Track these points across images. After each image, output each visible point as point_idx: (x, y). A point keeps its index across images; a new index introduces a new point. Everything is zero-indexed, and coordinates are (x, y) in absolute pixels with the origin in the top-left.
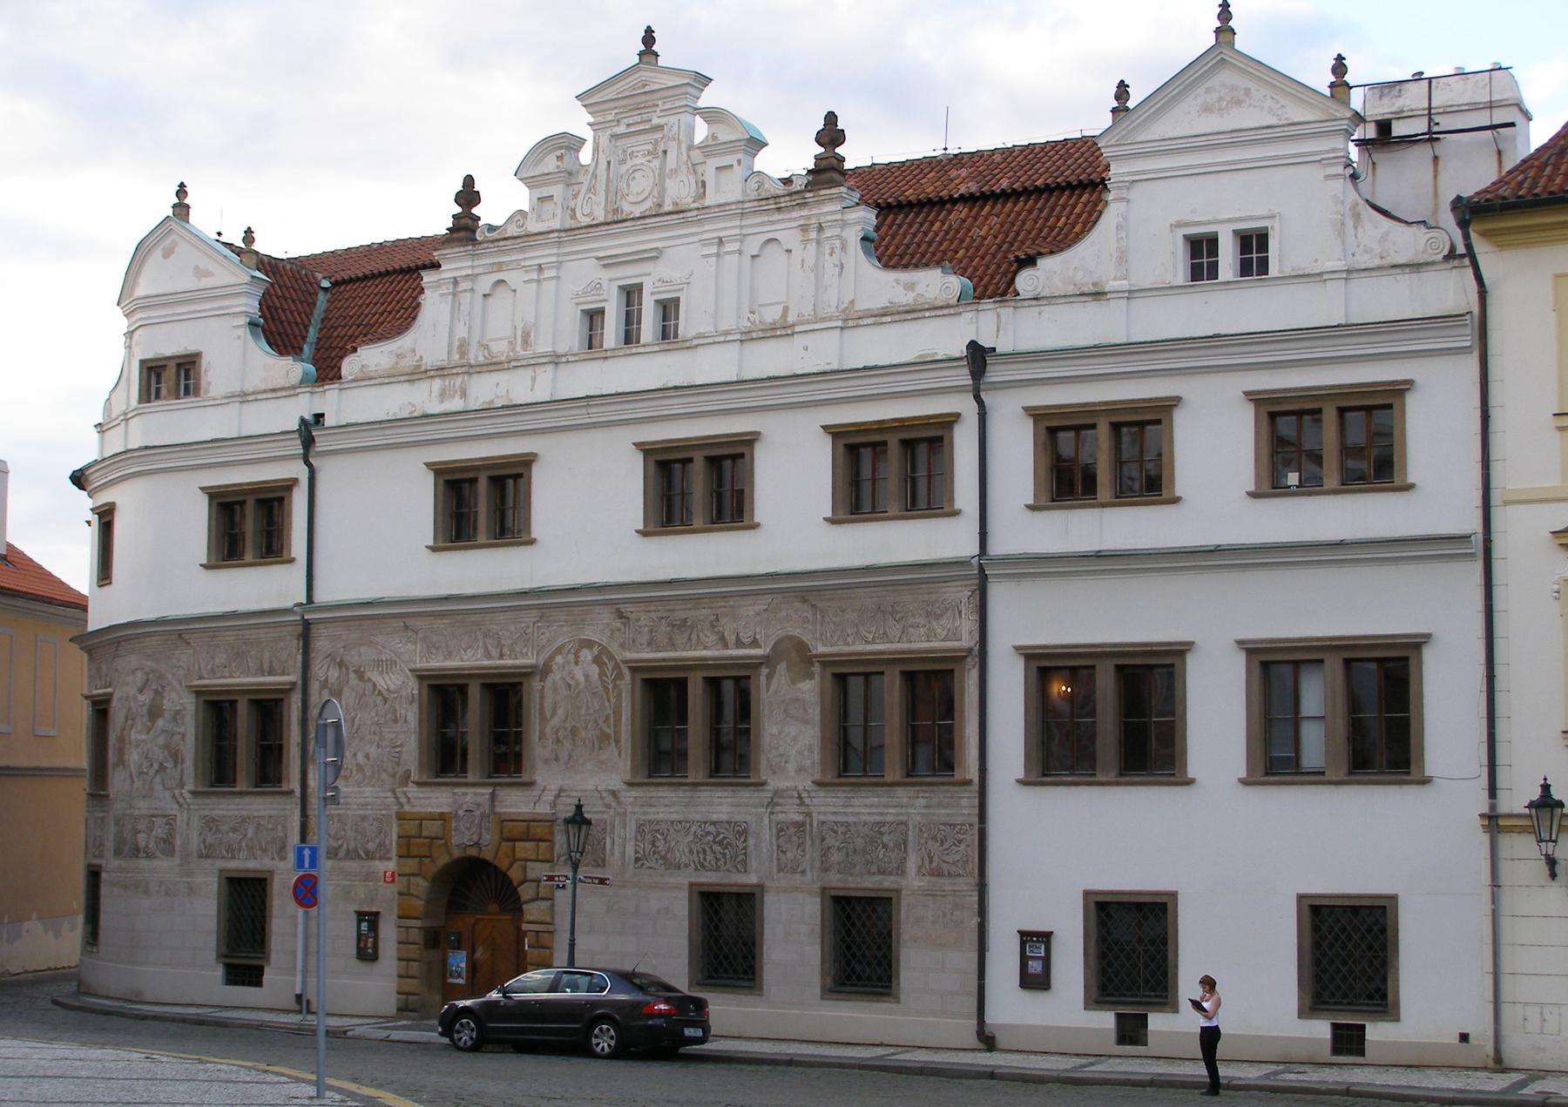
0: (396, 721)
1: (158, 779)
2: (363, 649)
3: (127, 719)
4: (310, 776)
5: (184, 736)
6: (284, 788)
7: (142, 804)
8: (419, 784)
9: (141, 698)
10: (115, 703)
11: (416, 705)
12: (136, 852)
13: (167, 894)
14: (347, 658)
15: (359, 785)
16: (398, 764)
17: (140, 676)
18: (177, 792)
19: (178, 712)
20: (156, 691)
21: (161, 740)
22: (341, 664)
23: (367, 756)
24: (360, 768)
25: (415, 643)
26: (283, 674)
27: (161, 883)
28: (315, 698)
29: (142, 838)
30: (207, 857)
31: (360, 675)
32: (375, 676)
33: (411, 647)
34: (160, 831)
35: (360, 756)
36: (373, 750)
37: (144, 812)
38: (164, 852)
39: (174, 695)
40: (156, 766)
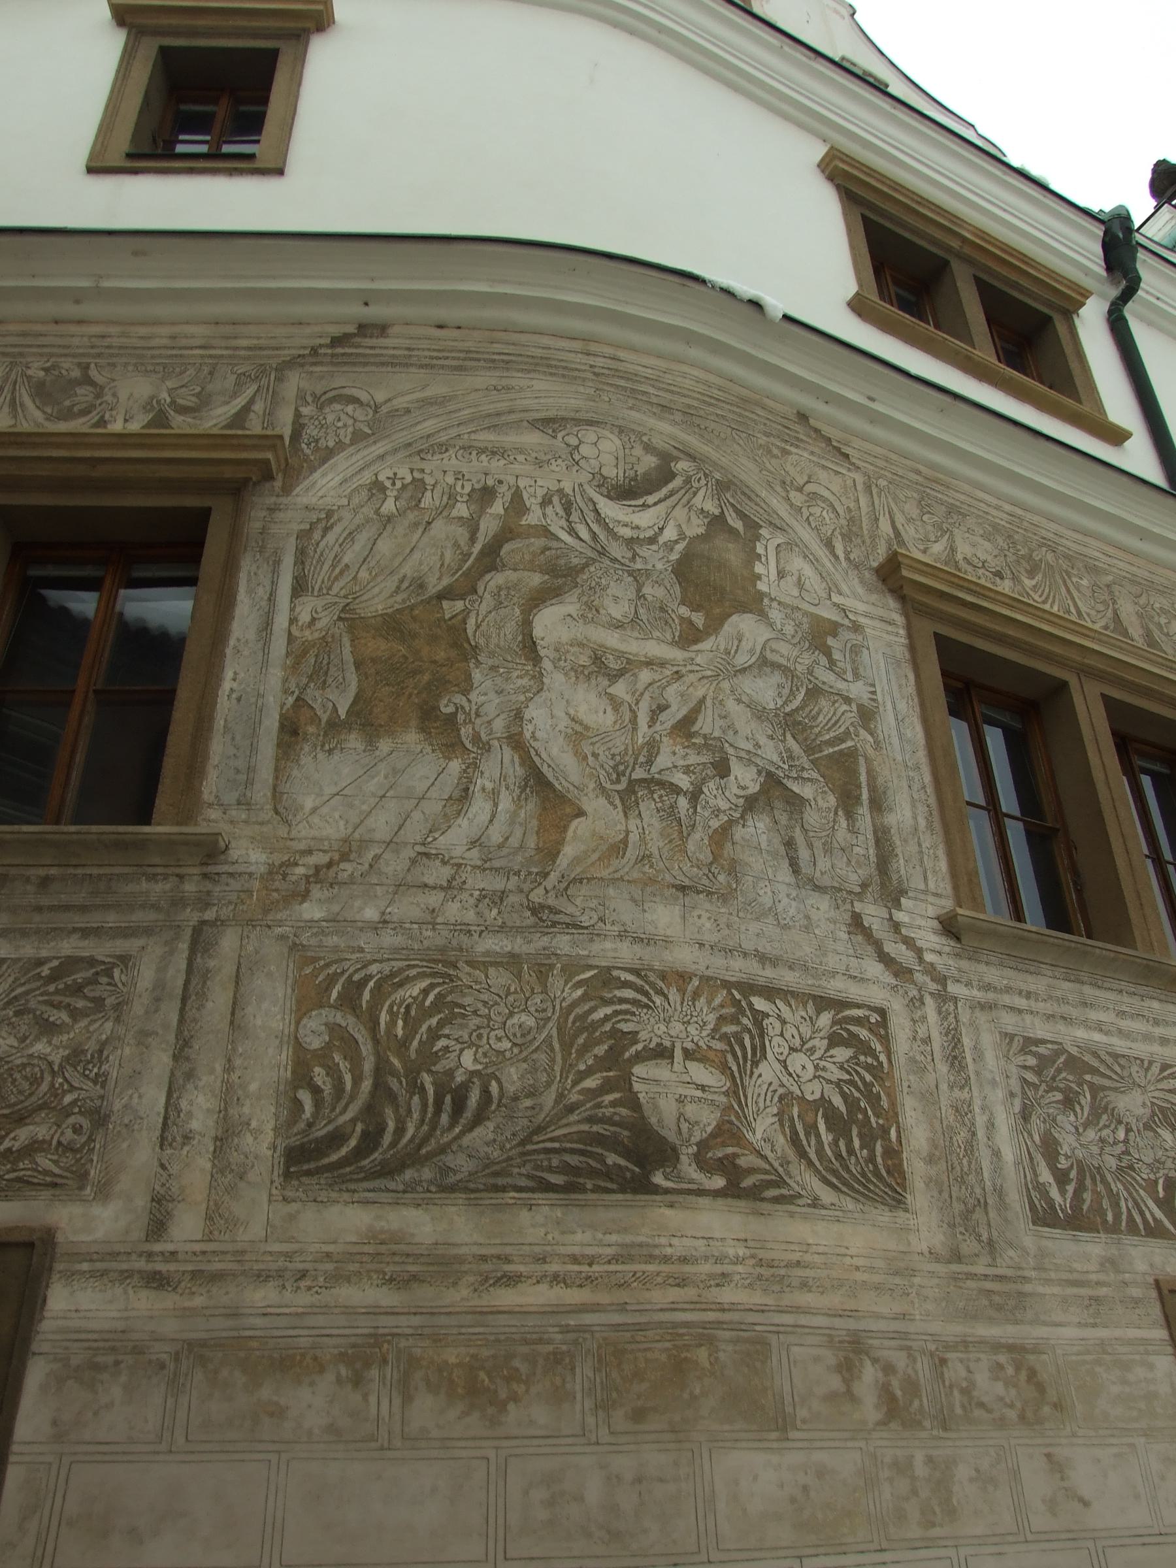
1: (758, 830)
3: (491, 559)
5: (867, 716)
7: (664, 917)
9: (611, 510)
10: (324, 486)
12: (634, 1159)
13: (894, 1409)
17: (604, 452)
18: (873, 913)
19: (834, 629)
20: (717, 522)
21: (765, 690)
27: (852, 1351)
29: (677, 1094)
30: (1077, 1221)
34: (798, 1062)
37: (684, 957)
38: (837, 1176)
39: (797, 564)
40: (745, 778)
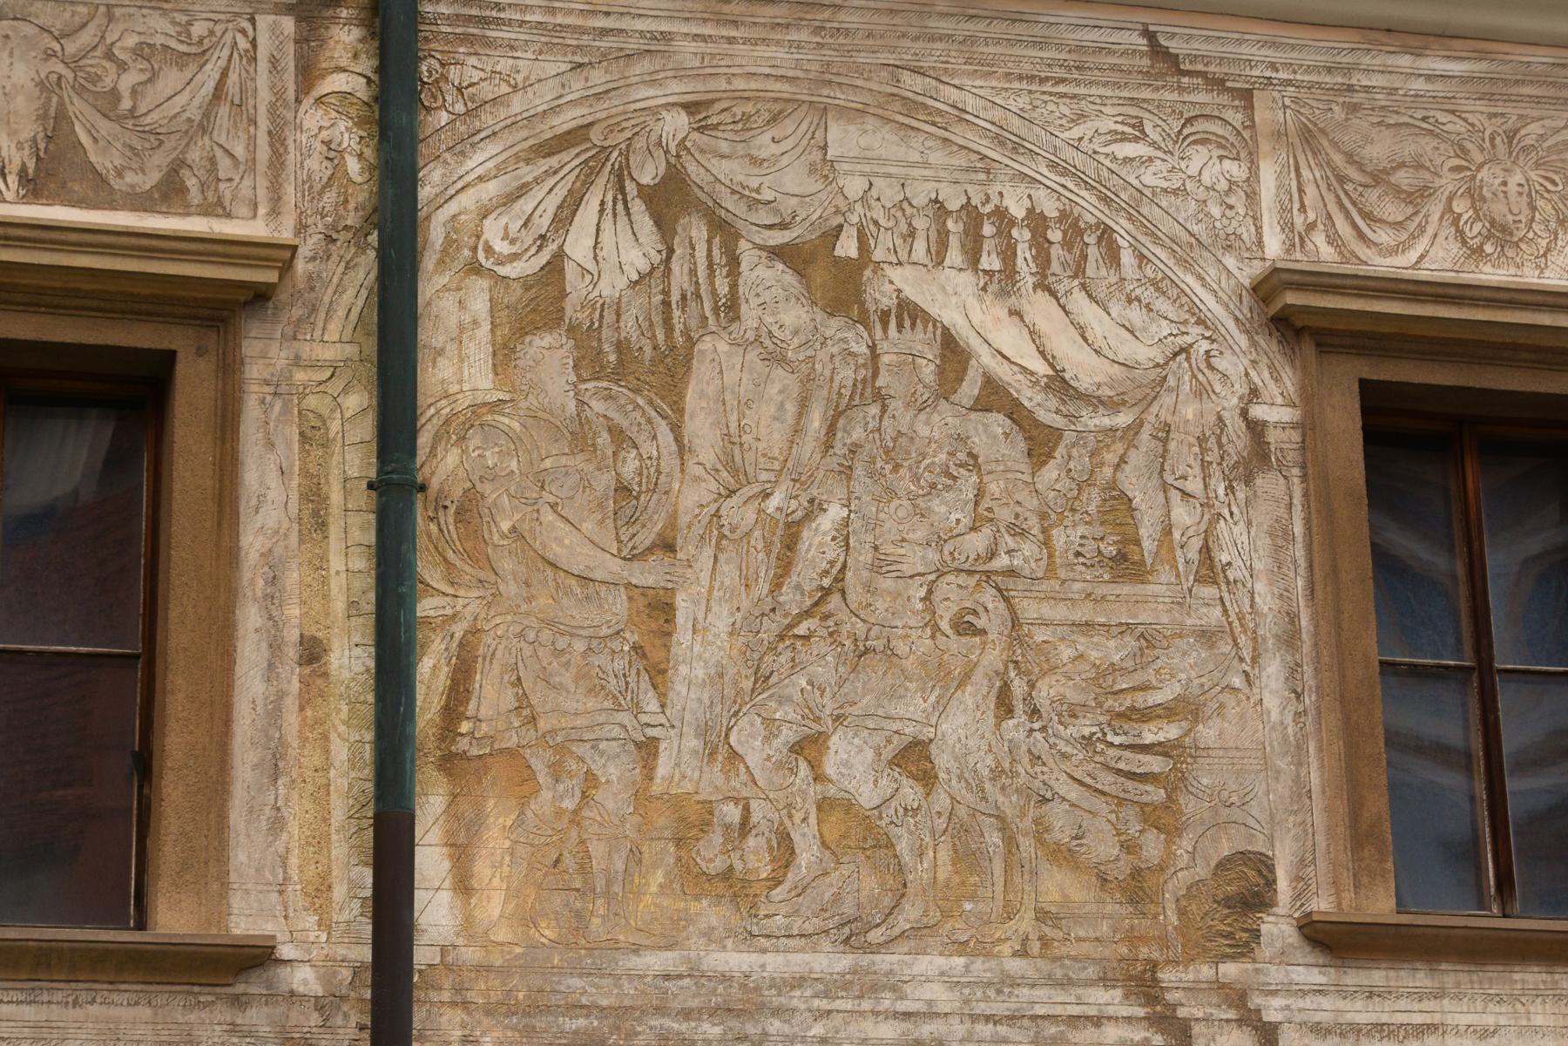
0: (1126, 564)
2: (842, 138)
4: (430, 861)
6: (173, 919)
8: (1333, 941)
11: (1280, 494)
14: (719, 170)
15: (852, 934)
16: (1164, 819)
22: (670, 200)
23: (914, 758)
24: (862, 834)
25: (1245, 147)
26: (170, 193)
28: (458, 364)
31: (833, 277)
32: (955, 298)
33: (1208, 167)
35: (853, 763)
36: (962, 730)
